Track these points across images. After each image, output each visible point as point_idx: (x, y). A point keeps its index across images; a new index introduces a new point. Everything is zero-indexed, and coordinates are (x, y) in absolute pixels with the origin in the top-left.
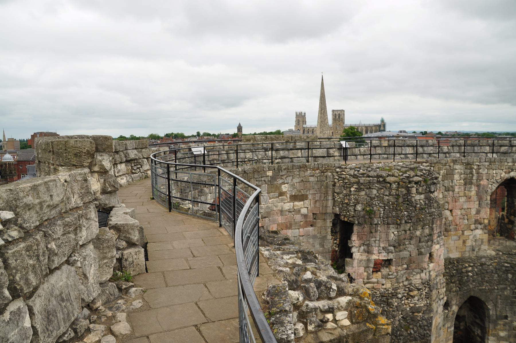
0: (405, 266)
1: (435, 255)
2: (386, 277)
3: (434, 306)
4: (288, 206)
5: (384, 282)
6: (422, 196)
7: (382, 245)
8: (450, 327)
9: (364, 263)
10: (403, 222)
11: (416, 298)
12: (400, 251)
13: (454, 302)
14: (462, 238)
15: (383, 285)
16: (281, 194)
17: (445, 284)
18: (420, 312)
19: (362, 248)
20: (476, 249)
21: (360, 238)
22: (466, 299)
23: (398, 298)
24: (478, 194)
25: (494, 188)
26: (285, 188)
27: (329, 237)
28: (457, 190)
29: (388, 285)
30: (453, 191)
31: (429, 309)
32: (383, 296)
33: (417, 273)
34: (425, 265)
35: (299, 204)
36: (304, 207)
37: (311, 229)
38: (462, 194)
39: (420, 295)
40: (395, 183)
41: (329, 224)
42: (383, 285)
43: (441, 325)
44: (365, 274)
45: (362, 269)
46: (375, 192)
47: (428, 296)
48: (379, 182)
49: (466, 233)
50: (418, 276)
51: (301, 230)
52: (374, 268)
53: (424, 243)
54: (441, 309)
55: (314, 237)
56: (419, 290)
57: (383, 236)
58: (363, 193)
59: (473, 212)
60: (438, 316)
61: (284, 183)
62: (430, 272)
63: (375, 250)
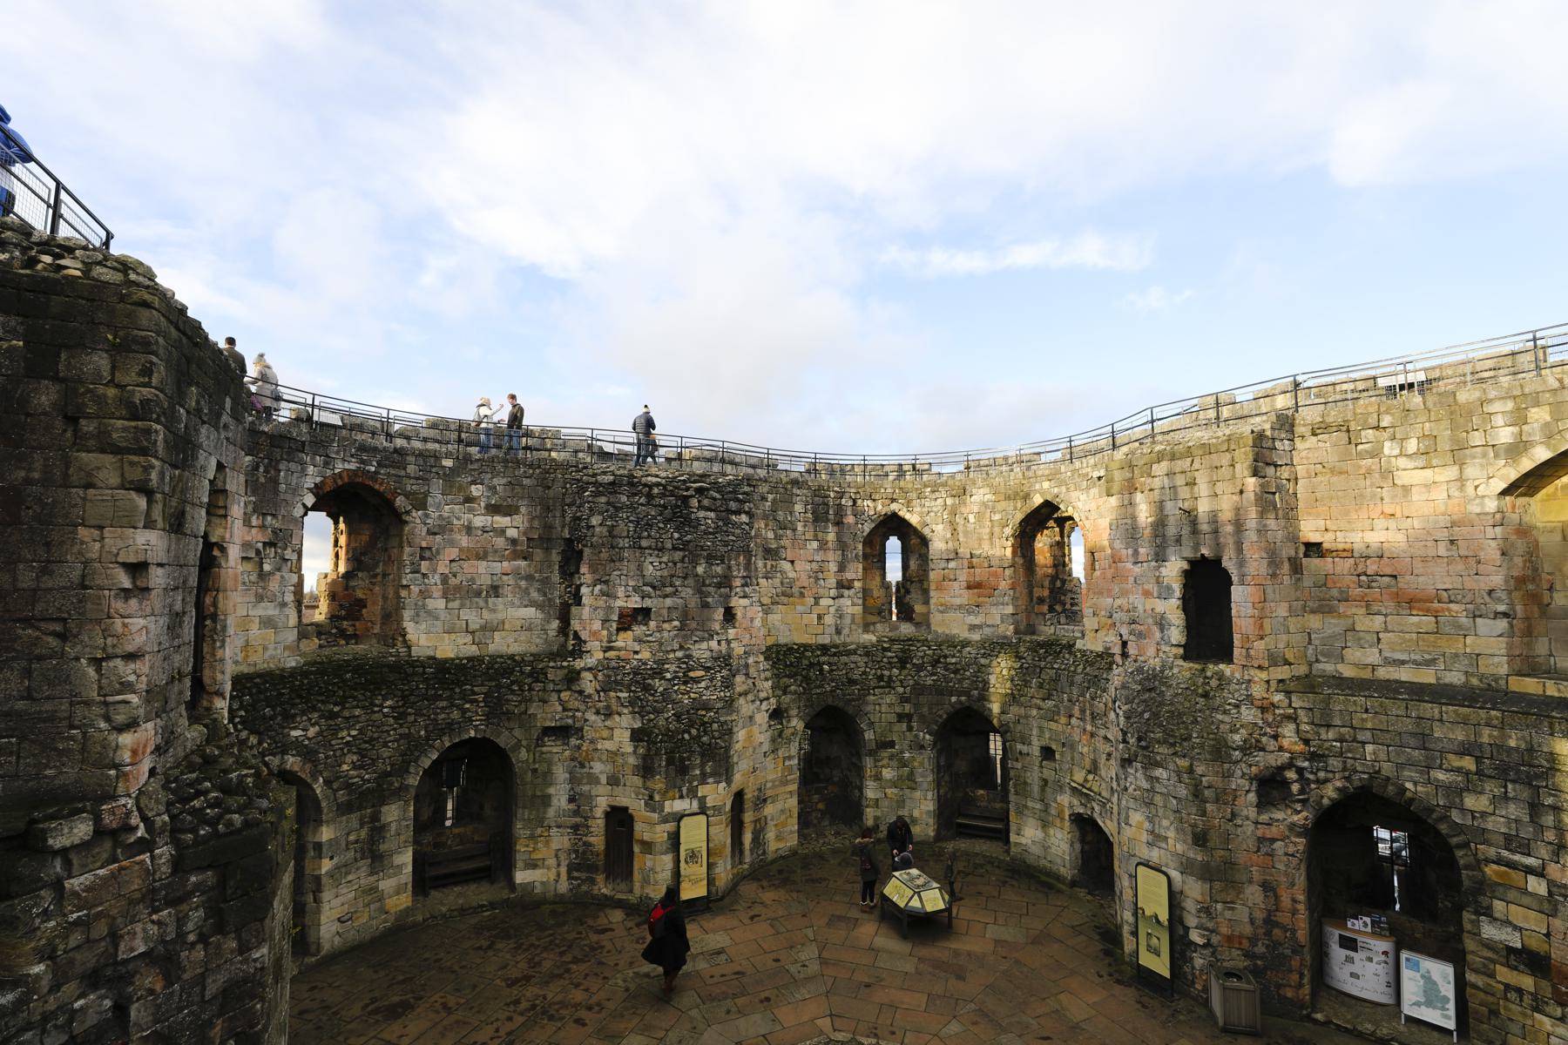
0: (676, 623)
1: (739, 615)
2: (640, 641)
3: (744, 706)
4: (479, 521)
5: (637, 648)
6: (712, 515)
7: (631, 583)
8: (790, 758)
9: (601, 614)
10: (669, 546)
11: (703, 684)
12: (666, 596)
13: (794, 712)
14: (816, 610)
15: (636, 653)
16: (469, 499)
17: (768, 674)
18: (710, 710)
19: (598, 587)
20: (846, 631)
21: (593, 570)
22: (817, 710)
23: (664, 678)
24: (839, 539)
25: (867, 530)
26: (476, 490)
27: (556, 577)
28: (800, 527)
29: (645, 655)
30: (794, 530)
31: (730, 704)
32: (636, 674)
33: (702, 640)
34: (717, 627)
35: (501, 521)
36: (513, 526)
37: (523, 563)
38: (809, 535)
39: (711, 680)
40: (658, 485)
41: (556, 557)
42: (636, 653)
43: (766, 747)
44: (605, 632)
45: (597, 625)
46: (624, 499)
47: (728, 684)
48: (631, 484)
49: (823, 602)
50: (704, 645)
51: (505, 564)
52: (619, 622)
53: (711, 589)
54: (762, 718)
55: (529, 578)
56: (707, 669)
57: (633, 567)
58: (603, 499)
59: (833, 567)
60: (755, 729)
61: (474, 483)
62: (728, 642)
63: (621, 592)
